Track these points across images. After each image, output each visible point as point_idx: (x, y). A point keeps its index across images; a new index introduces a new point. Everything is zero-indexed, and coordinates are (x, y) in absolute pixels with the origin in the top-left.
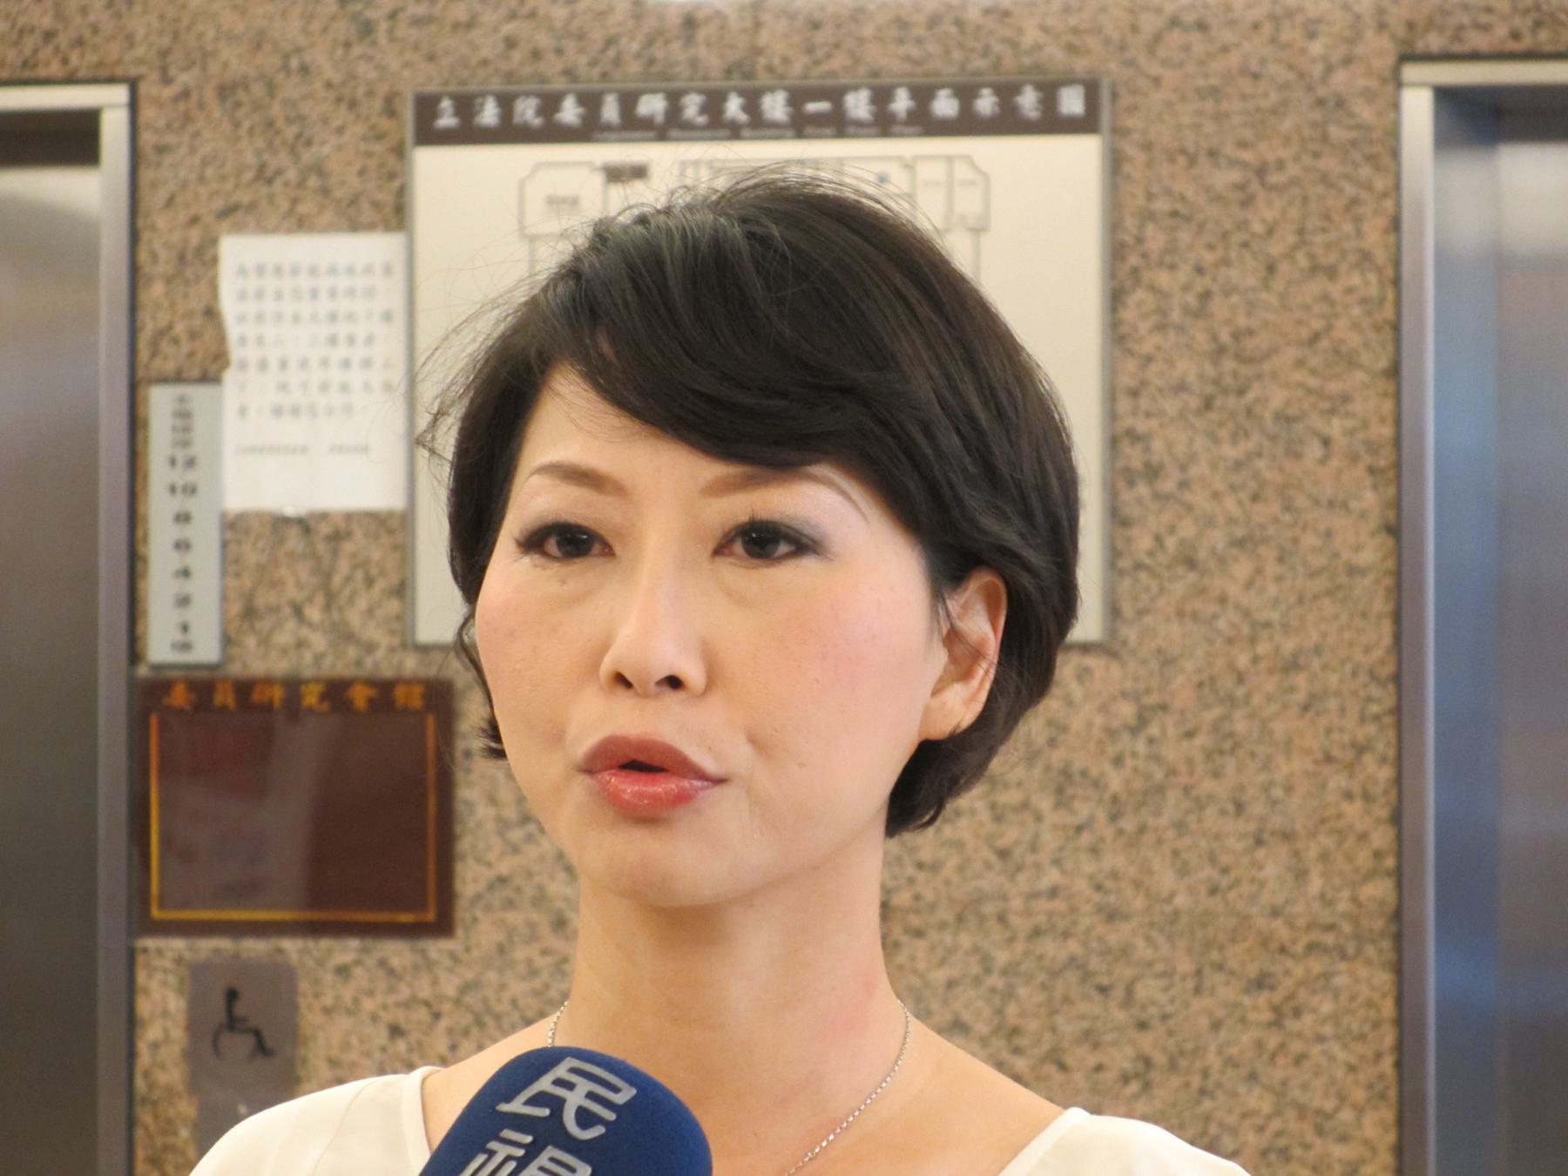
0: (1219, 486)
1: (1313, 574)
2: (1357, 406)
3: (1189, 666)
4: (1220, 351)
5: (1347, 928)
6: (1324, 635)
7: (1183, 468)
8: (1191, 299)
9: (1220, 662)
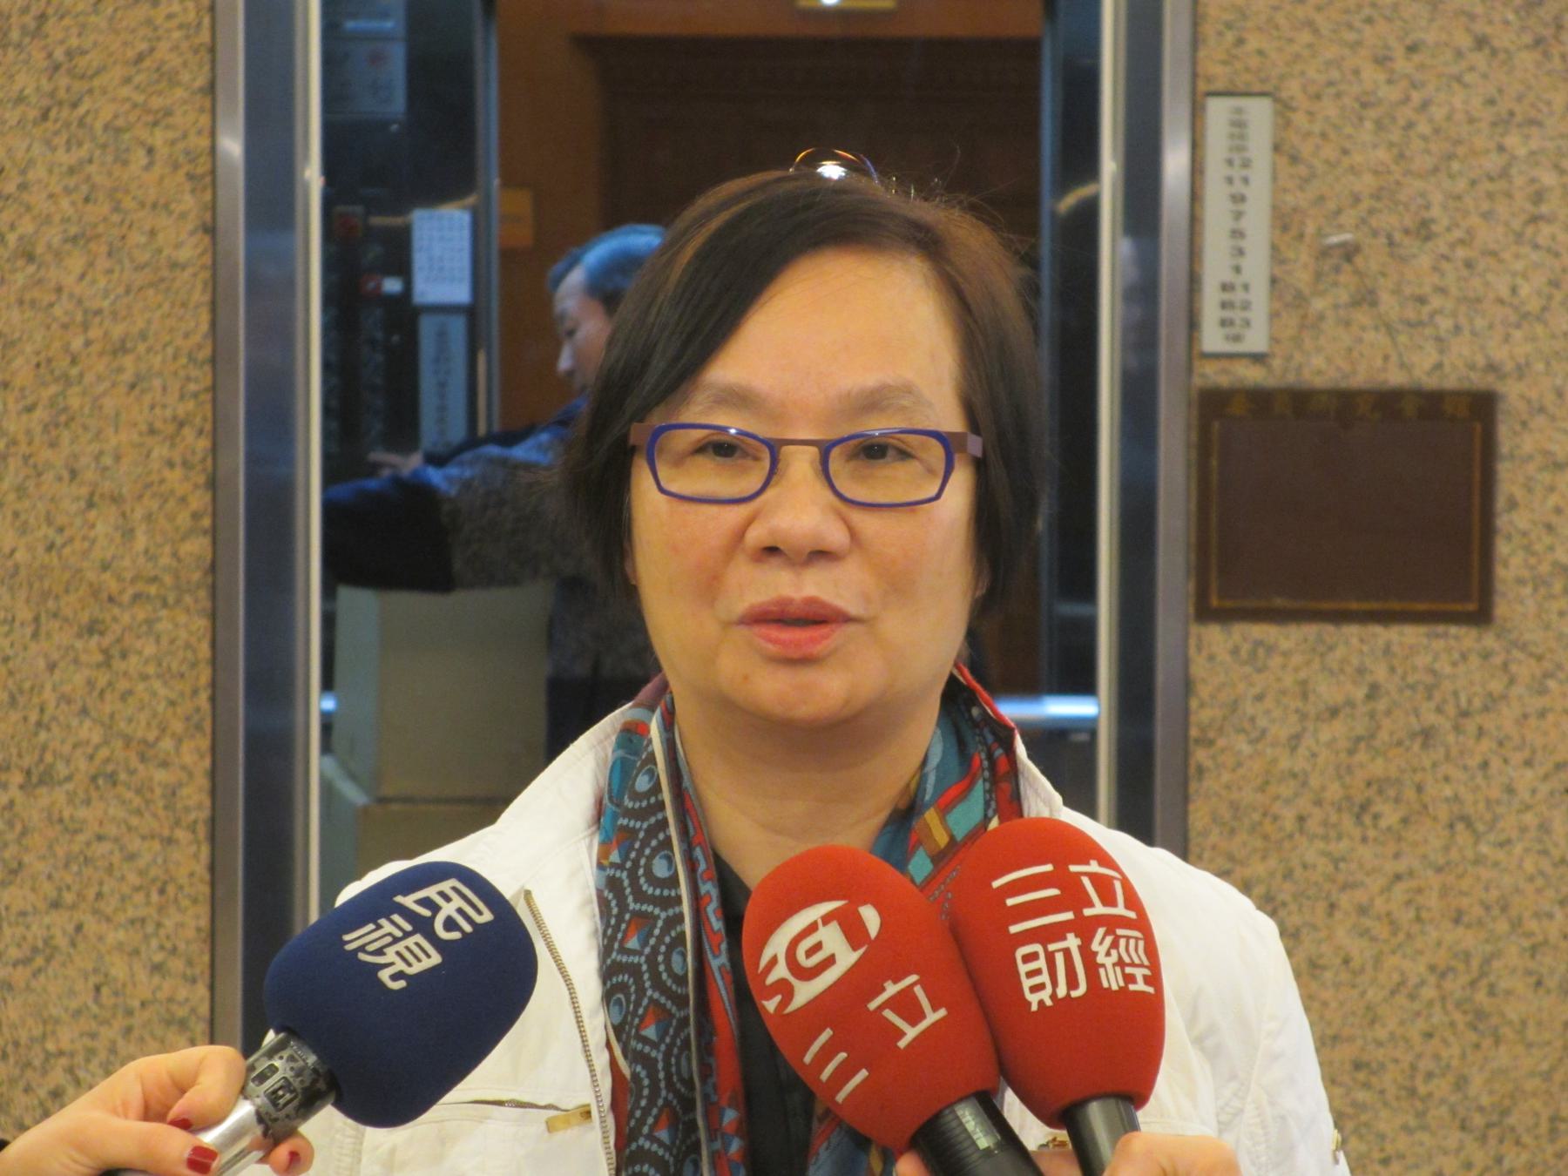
0: (58, 189)
1: (140, 268)
2: (178, 119)
3: (29, 349)
4: (57, 68)
5: (168, 580)
6: (149, 322)
7: (23, 172)
8: (29, 20)
9: (57, 344)
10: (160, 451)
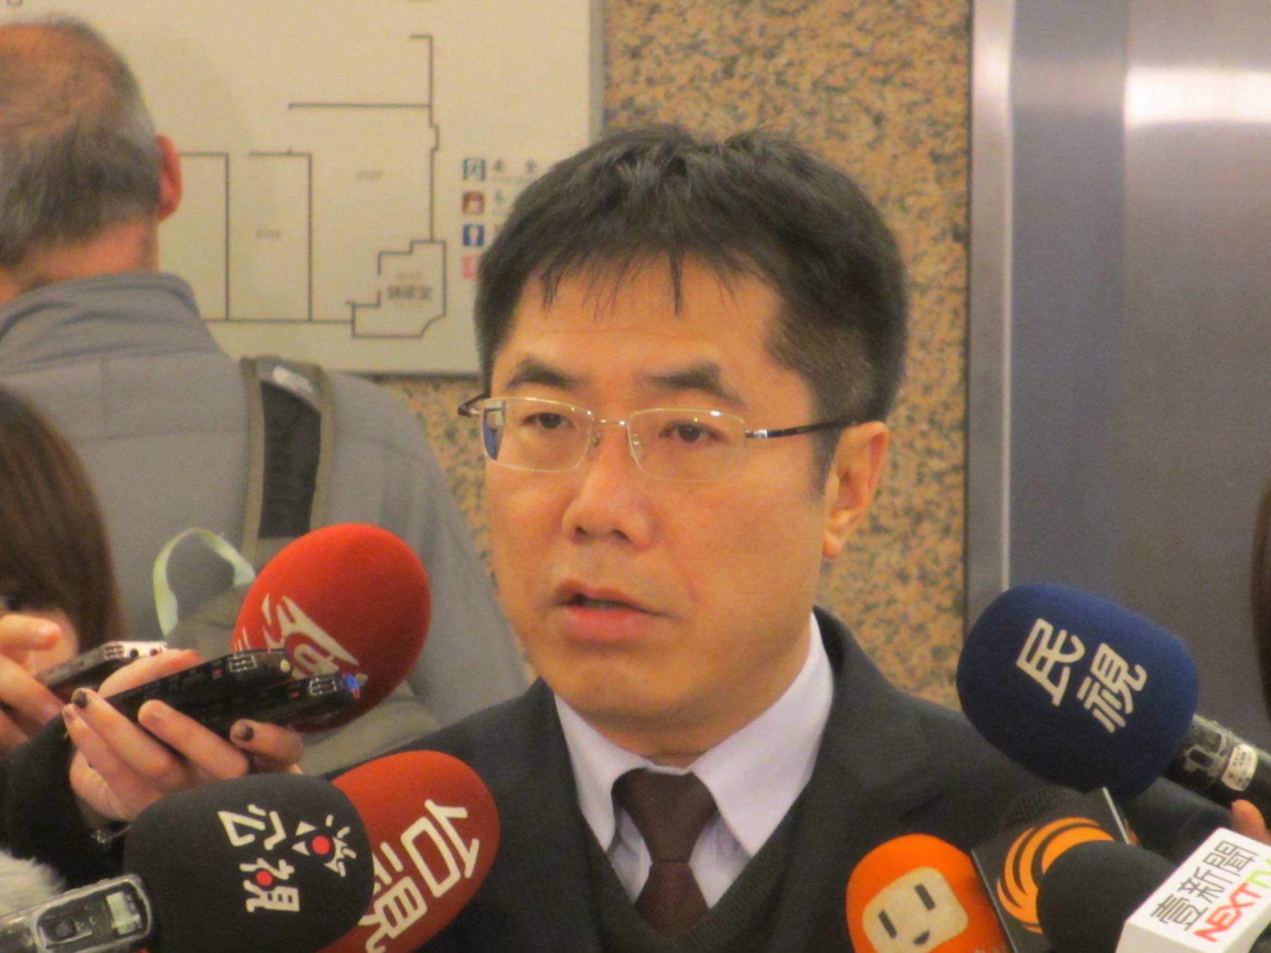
2: (918, 74)
10: (888, 557)
